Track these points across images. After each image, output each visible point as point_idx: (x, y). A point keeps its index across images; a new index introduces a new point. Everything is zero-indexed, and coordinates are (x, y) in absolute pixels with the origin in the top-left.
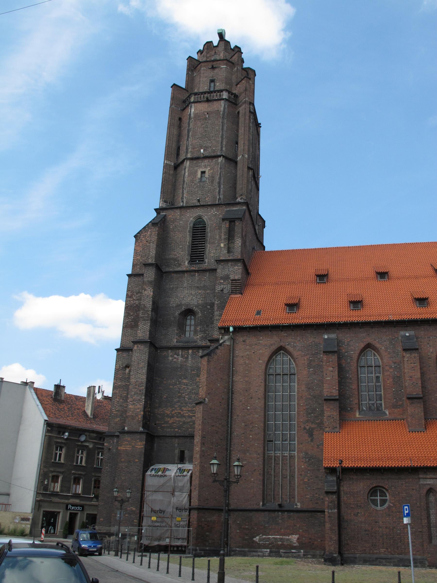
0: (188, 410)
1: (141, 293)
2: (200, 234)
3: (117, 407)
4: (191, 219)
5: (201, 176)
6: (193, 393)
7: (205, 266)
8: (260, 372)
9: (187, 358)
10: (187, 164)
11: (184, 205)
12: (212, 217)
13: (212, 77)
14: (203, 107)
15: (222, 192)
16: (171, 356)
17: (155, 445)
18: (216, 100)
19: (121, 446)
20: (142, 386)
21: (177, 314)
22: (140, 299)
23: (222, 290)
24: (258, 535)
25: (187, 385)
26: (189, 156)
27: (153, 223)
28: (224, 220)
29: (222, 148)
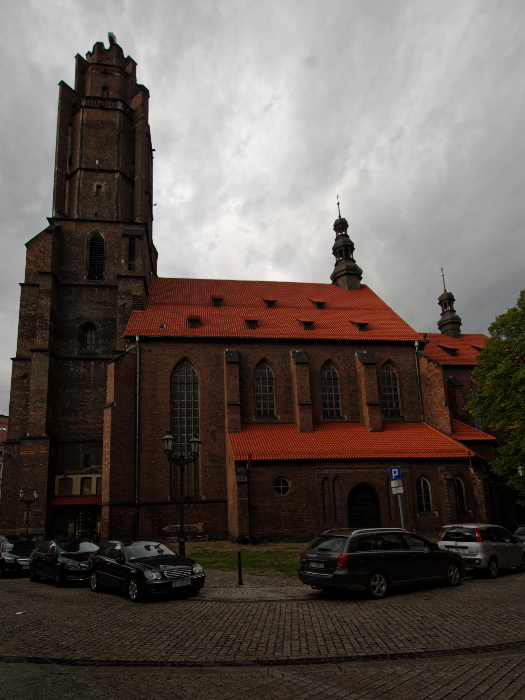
0: (92, 418)
4: (88, 233)
5: (97, 190)
7: (105, 282)
9: (90, 369)
11: (80, 218)
14: (97, 115)
16: (73, 367)
18: (110, 109)
21: (77, 326)
22: (36, 310)
23: (124, 305)
24: (166, 525)
25: (90, 395)
26: (83, 166)
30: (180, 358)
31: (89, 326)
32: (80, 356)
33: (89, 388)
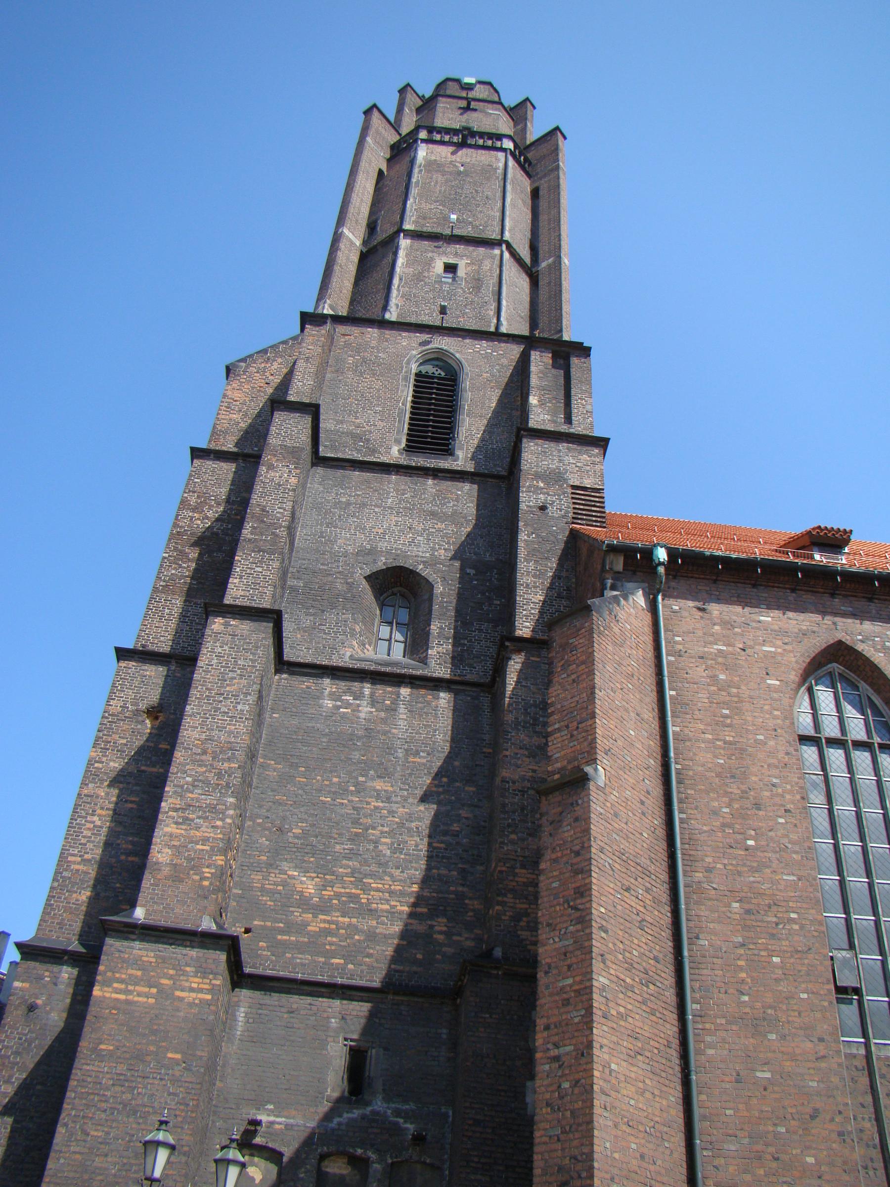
0: (391, 893)
3: (90, 846)
6: (409, 830)
8: (776, 718)
9: (392, 709)
10: (404, 243)
16: (333, 696)
17: (241, 1015)
25: (388, 800)
33: (384, 774)
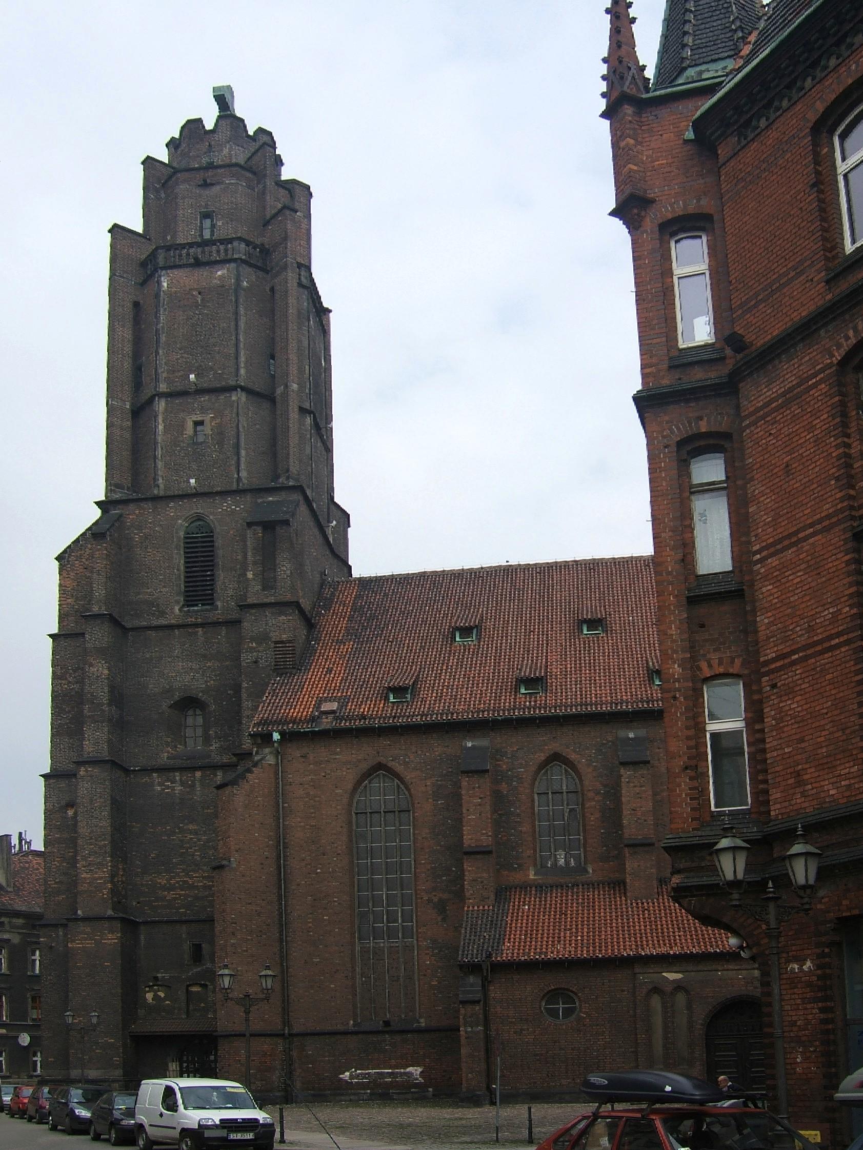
1: (83, 669)
2: (202, 552)
12: (226, 517)
13: (207, 206)
15: (242, 466)
19: (73, 941)
20: (103, 840)
21: (165, 705)
23: (256, 662)
27: (94, 534)
28: (250, 525)
29: (237, 370)
30: (365, 766)
31: (189, 703)
32: (172, 762)
